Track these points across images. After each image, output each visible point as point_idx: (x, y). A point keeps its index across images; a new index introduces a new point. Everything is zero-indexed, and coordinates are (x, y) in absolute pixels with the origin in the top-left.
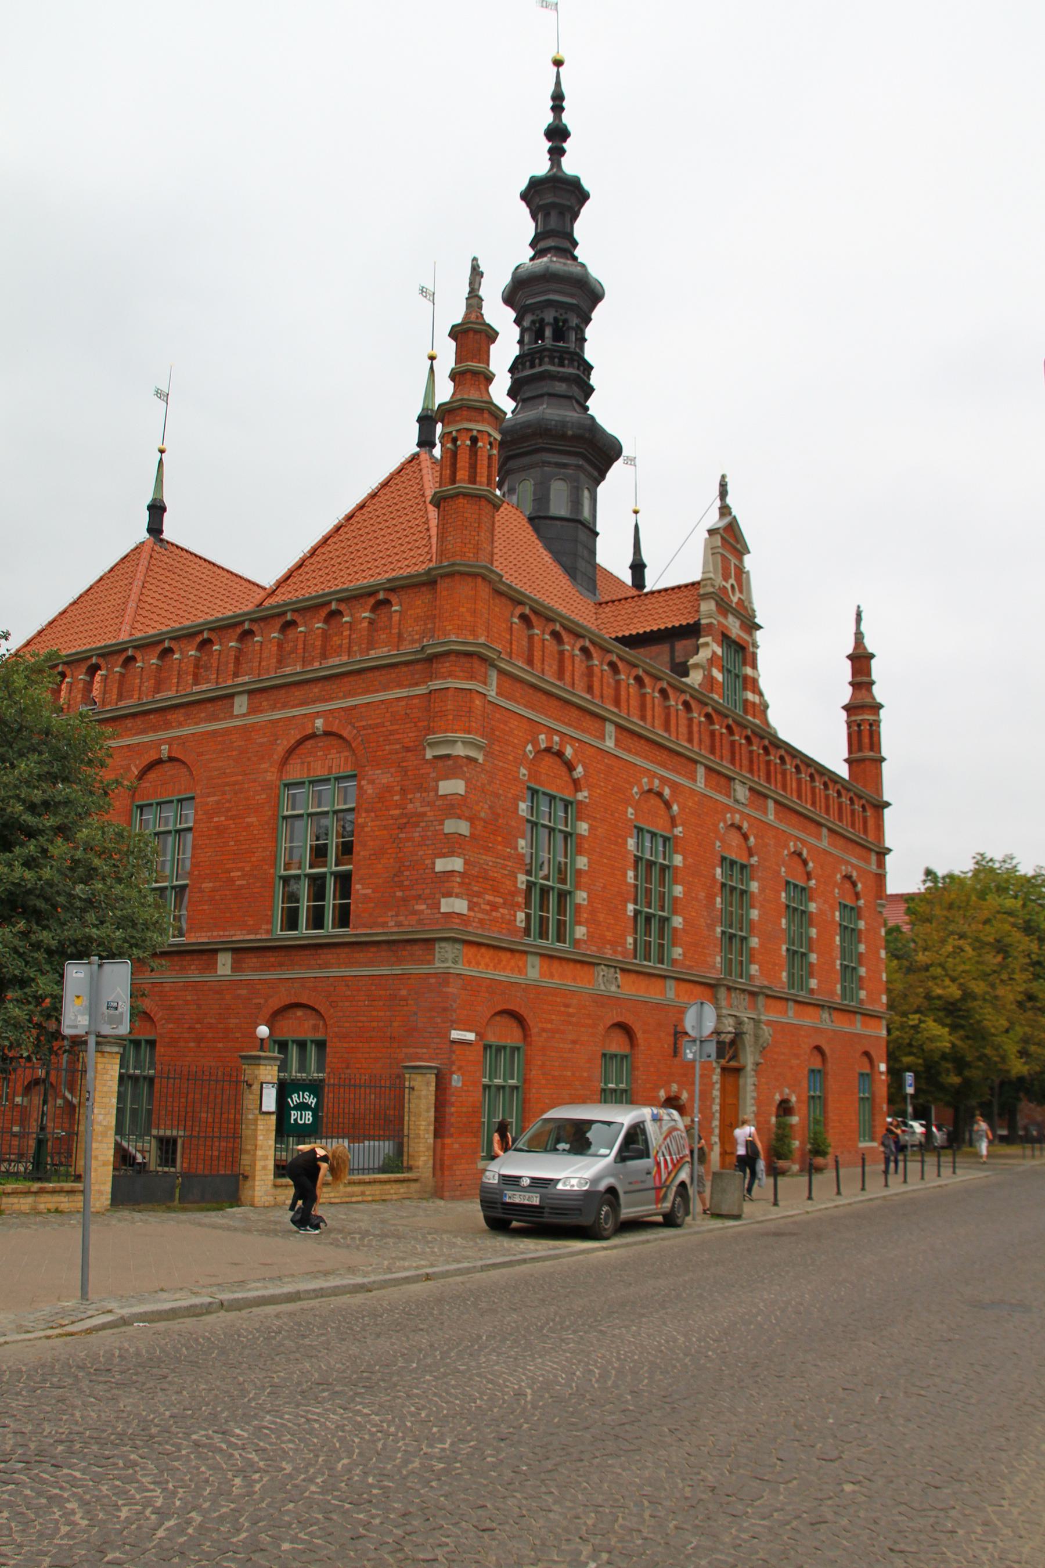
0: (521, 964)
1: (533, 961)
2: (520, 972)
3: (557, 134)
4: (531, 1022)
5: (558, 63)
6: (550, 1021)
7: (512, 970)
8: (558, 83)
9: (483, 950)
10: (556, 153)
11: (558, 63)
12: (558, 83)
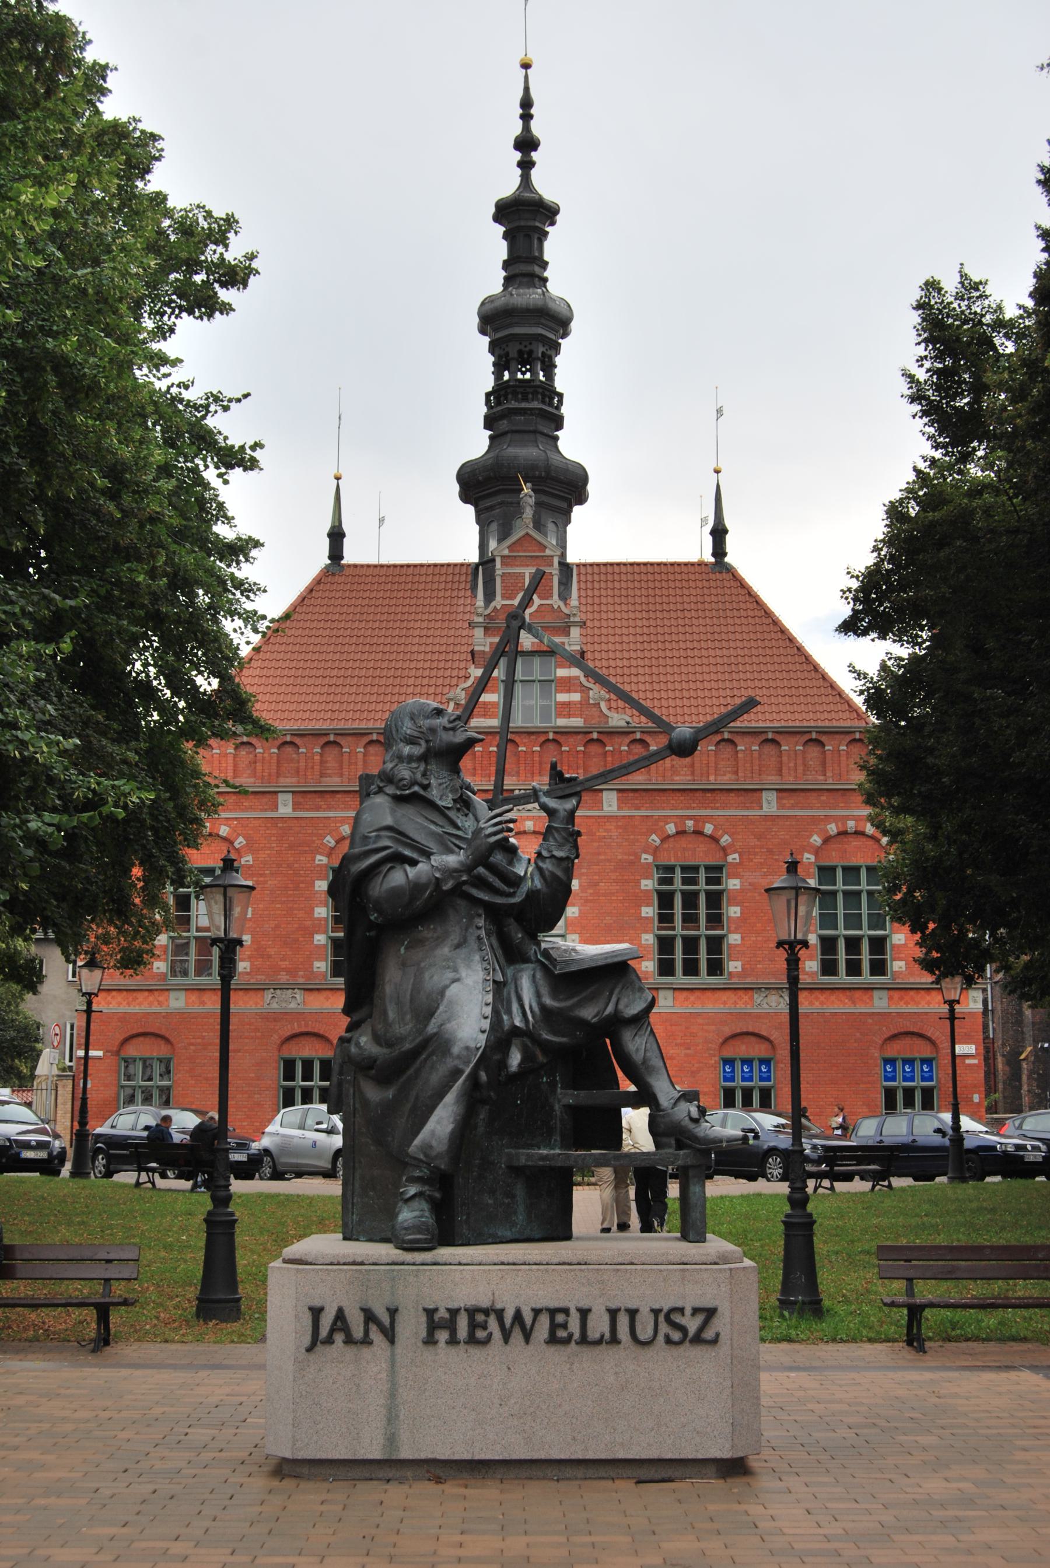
0: (161, 999)
1: (182, 995)
2: (160, 1004)
3: (526, 144)
4: (172, 1039)
5: (526, 66)
6: (203, 1038)
7: (151, 1004)
8: (527, 89)
9: (114, 993)
10: (526, 165)
11: (526, 66)
12: (527, 89)
